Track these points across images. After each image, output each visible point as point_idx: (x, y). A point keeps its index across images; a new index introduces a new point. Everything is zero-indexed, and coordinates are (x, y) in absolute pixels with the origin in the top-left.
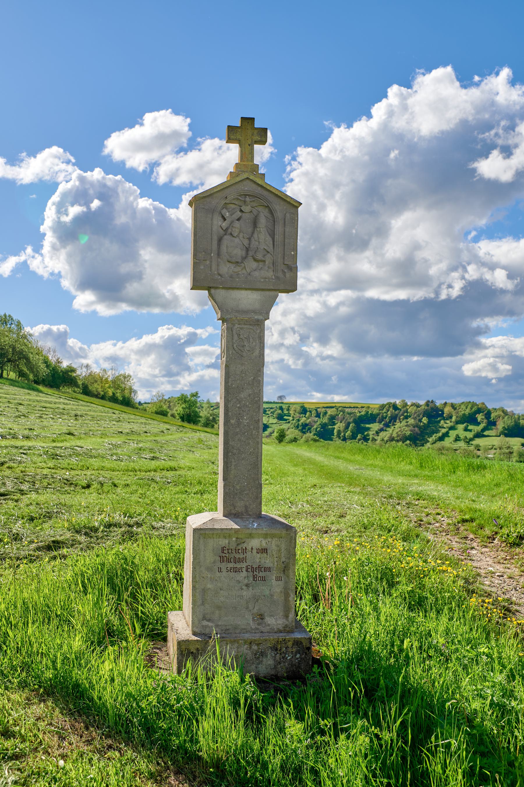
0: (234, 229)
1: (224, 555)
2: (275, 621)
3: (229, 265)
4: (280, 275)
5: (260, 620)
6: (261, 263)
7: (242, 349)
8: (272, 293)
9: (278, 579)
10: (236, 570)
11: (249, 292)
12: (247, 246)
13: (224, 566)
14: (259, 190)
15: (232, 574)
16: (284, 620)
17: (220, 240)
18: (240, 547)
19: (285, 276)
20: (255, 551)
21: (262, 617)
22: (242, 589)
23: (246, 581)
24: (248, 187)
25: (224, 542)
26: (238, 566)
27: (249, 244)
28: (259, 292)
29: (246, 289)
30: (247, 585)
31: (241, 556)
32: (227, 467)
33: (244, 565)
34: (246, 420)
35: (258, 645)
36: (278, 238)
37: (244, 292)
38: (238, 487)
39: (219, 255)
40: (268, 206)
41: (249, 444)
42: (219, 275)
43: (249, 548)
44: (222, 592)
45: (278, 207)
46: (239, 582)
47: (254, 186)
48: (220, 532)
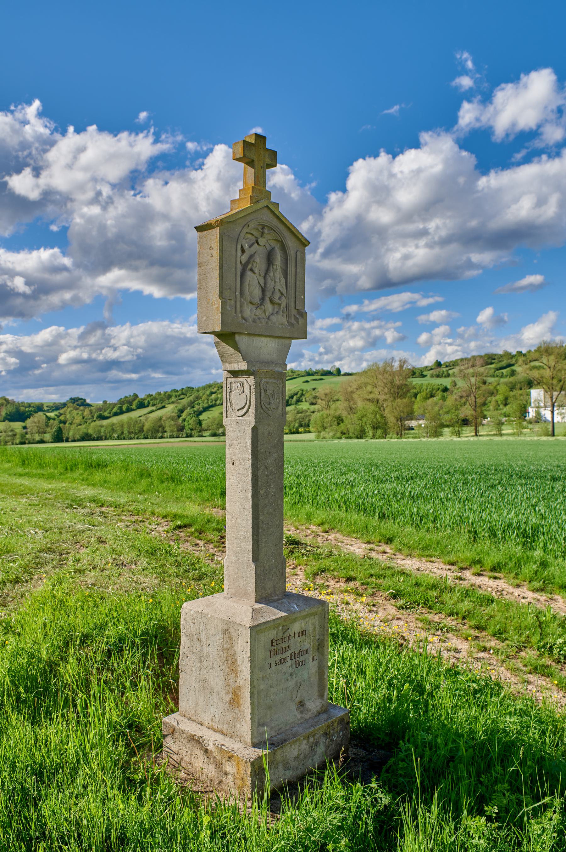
0: (255, 264)
1: (273, 648)
2: (314, 705)
3: (251, 306)
4: (293, 320)
5: (302, 708)
6: (276, 306)
7: (268, 406)
8: (286, 341)
9: (314, 659)
10: (282, 661)
11: (268, 339)
12: (263, 285)
13: (272, 660)
14: (275, 222)
15: (280, 667)
16: (320, 700)
17: (242, 275)
18: (285, 636)
19: (298, 322)
20: (296, 636)
21: (302, 704)
22: (287, 680)
23: (290, 671)
24: (267, 217)
25: (272, 634)
26: (284, 656)
27: (265, 284)
28: (276, 340)
29: (266, 336)
30: (291, 675)
31: (286, 645)
32: (258, 546)
33: (288, 654)
34: (273, 488)
35: (314, 736)
36: (291, 278)
37: (263, 339)
38: (267, 567)
39: (242, 294)
40: (282, 241)
41: (275, 516)
42: (243, 318)
43: (292, 634)
44: (272, 689)
45: (291, 243)
46: (285, 673)
47: (271, 216)
48: (272, 624)
